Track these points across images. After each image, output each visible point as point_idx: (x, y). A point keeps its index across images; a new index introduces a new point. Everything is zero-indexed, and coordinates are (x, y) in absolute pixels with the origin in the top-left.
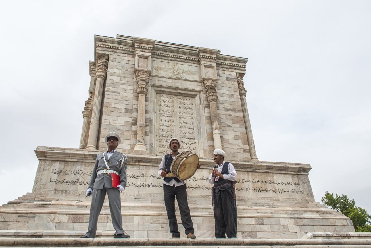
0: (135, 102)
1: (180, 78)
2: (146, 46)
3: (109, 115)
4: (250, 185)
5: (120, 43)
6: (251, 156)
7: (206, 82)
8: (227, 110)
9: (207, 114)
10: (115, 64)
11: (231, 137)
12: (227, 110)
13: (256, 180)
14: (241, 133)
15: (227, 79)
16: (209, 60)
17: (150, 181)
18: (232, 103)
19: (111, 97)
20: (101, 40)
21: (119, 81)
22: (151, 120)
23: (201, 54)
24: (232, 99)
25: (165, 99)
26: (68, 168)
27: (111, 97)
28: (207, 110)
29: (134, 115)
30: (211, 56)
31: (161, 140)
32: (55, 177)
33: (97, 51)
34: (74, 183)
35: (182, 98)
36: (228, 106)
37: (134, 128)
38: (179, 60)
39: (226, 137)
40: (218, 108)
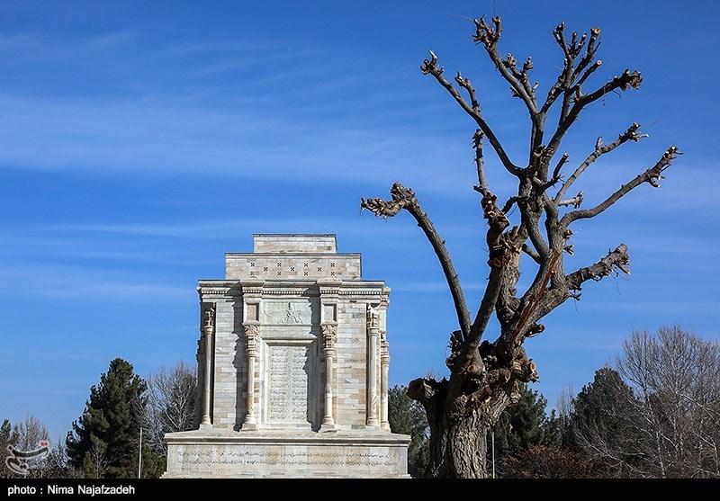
0: (245, 364)
1: (295, 323)
2: (254, 288)
3: (219, 381)
4: (345, 459)
5: (225, 286)
6: (367, 416)
7: (324, 328)
8: (347, 361)
9: (322, 371)
10: (223, 315)
11: (347, 396)
12: (347, 361)
13: (351, 453)
14: (360, 390)
15: (353, 317)
16: (330, 295)
17: (255, 458)
18: (354, 351)
19: (221, 359)
20: (206, 286)
21: (229, 339)
22: (263, 382)
23: (321, 288)
24: (356, 346)
25: (279, 350)
26: (190, 449)
27: (221, 359)
28: (322, 363)
29: (244, 379)
30: (334, 289)
31: (272, 404)
32: (181, 458)
33: (204, 301)
34: (195, 462)
35: (297, 348)
36: (350, 356)
37: (244, 393)
38: (295, 296)
39: (340, 396)
40: (335, 361)
